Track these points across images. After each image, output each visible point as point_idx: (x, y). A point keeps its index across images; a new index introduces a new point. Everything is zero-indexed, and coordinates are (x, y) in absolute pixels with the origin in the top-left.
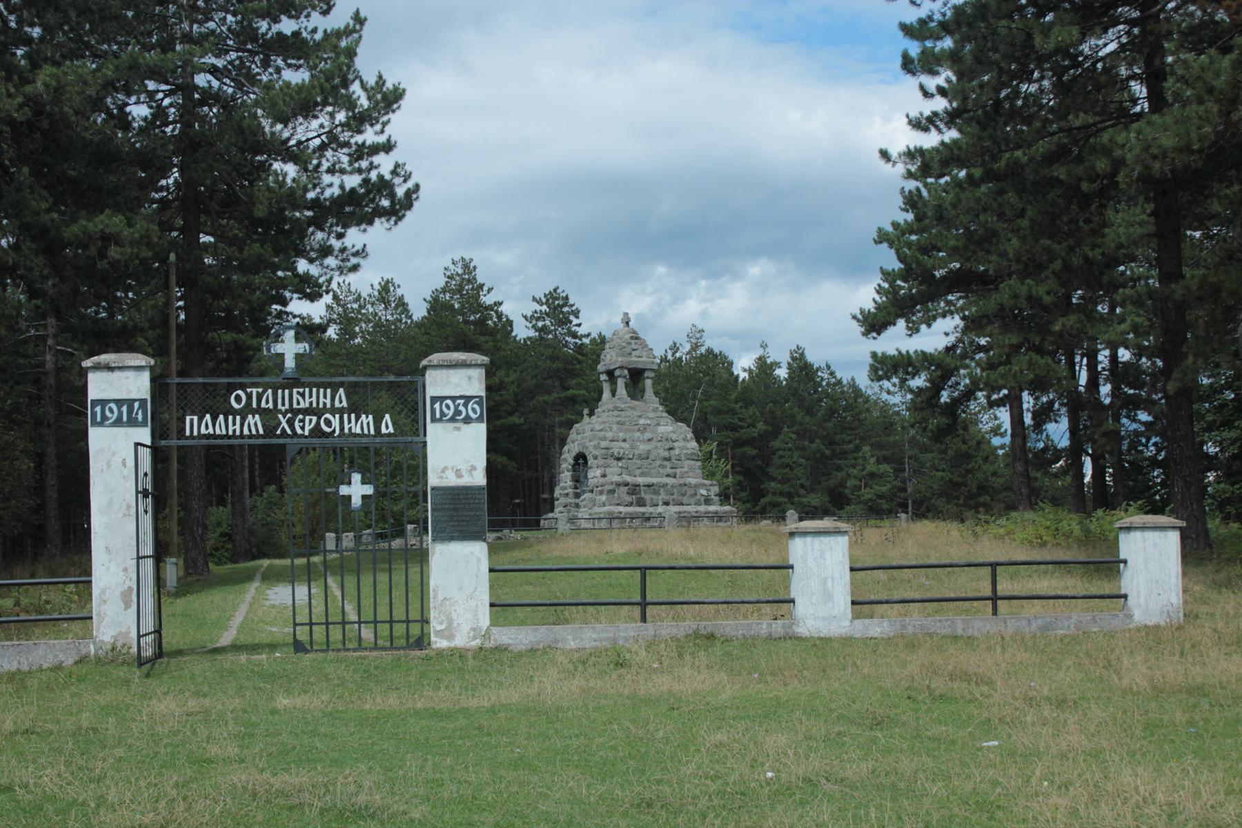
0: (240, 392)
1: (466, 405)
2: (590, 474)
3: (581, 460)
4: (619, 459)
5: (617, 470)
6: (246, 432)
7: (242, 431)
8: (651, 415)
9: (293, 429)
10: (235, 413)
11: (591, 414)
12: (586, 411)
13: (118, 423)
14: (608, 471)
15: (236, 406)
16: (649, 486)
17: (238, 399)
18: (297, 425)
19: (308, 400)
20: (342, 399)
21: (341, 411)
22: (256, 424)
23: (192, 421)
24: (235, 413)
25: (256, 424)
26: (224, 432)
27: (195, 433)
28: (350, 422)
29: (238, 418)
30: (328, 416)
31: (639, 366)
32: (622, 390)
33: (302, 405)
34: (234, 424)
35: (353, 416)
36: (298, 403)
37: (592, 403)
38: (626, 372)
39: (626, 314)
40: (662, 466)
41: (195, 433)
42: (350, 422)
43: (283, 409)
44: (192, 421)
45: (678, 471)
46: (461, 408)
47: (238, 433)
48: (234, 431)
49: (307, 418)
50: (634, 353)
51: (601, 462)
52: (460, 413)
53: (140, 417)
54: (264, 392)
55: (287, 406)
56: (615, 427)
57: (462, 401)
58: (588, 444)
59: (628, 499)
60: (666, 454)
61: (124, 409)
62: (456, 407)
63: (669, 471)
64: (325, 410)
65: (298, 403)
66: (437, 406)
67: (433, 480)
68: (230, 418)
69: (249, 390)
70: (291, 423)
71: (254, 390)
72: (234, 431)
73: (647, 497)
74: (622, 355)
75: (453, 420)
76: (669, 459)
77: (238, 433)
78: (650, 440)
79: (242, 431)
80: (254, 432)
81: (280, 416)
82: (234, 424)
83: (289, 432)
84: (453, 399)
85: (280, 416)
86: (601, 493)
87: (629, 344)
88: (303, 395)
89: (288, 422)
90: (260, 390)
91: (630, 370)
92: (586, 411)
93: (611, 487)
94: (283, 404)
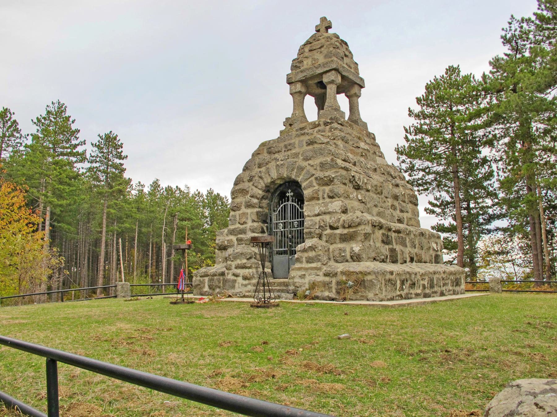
2: (308, 209)
4: (358, 188)
5: (356, 204)
8: (368, 141)
14: (349, 204)
16: (398, 232)
40: (393, 207)
45: (405, 215)
51: (340, 189)
56: (340, 143)
59: (385, 250)
60: (396, 191)
63: (397, 214)
73: (398, 248)
74: (336, 55)
76: (396, 197)
78: (375, 170)
86: (345, 239)
93: (368, 229)
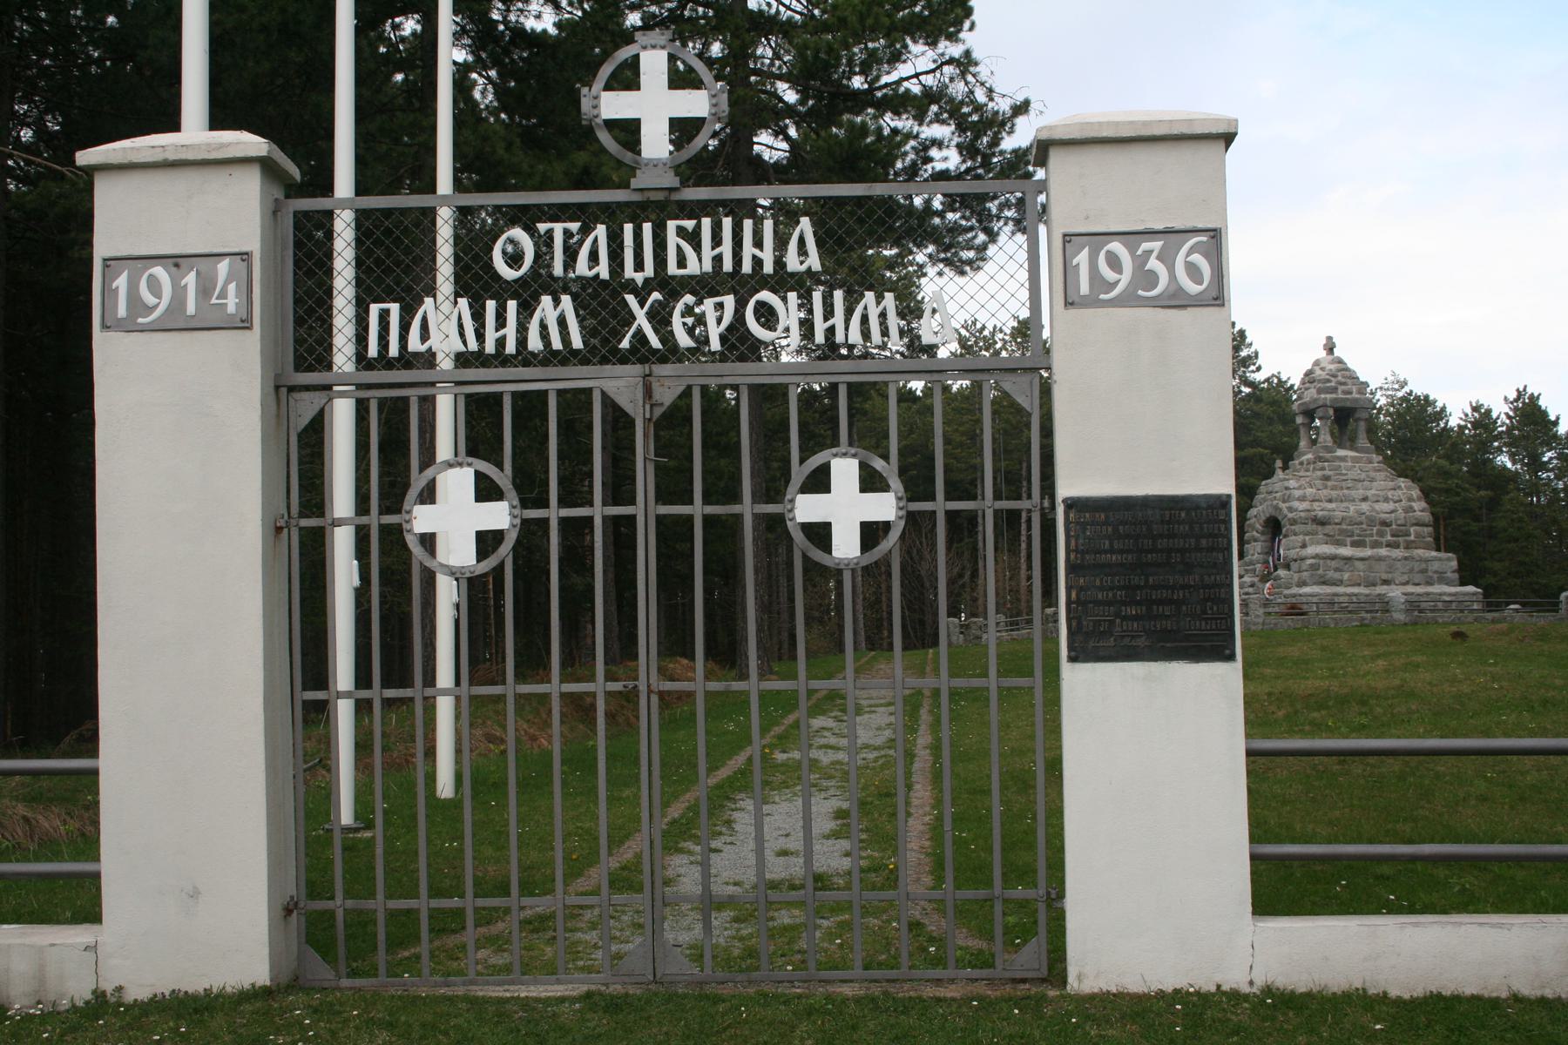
0: (517, 233)
1: (1166, 257)
3: (1274, 527)
6: (534, 343)
7: (522, 341)
9: (667, 337)
10: (502, 291)
11: (1285, 468)
12: (1279, 463)
13: (175, 323)
15: (508, 273)
17: (514, 260)
18: (677, 322)
19: (708, 253)
20: (805, 257)
21: (801, 284)
22: (562, 322)
23: (384, 316)
24: (502, 291)
25: (562, 322)
26: (473, 345)
27: (394, 351)
28: (829, 313)
29: (512, 305)
30: (765, 295)
31: (1348, 404)
32: (1326, 438)
33: (693, 268)
34: (501, 322)
35: (838, 295)
36: (682, 263)
37: (1288, 454)
38: (1331, 412)
39: (1329, 339)
41: (394, 351)
42: (829, 313)
43: (639, 278)
44: (384, 316)
46: (1153, 264)
47: (511, 348)
48: (501, 343)
49: (708, 305)
50: (1341, 388)
52: (1151, 279)
53: (232, 303)
54: (586, 230)
55: (649, 270)
57: (1156, 245)
58: (1282, 505)
61: (190, 279)
62: (1140, 261)
64: (759, 280)
65: (682, 263)
66: (1082, 259)
67: (1076, 479)
68: (491, 305)
69: (542, 227)
70: (660, 318)
71: (558, 228)
72: (501, 343)
75: (1128, 300)
77: (511, 348)
79: (522, 341)
80: (557, 344)
81: (631, 299)
82: (501, 322)
83: (655, 342)
84: (1131, 237)
85: (631, 299)
87: (1335, 376)
88: (694, 238)
89: (651, 316)
90: (574, 226)
91: (1336, 410)
92: (1279, 463)
94: (639, 266)
